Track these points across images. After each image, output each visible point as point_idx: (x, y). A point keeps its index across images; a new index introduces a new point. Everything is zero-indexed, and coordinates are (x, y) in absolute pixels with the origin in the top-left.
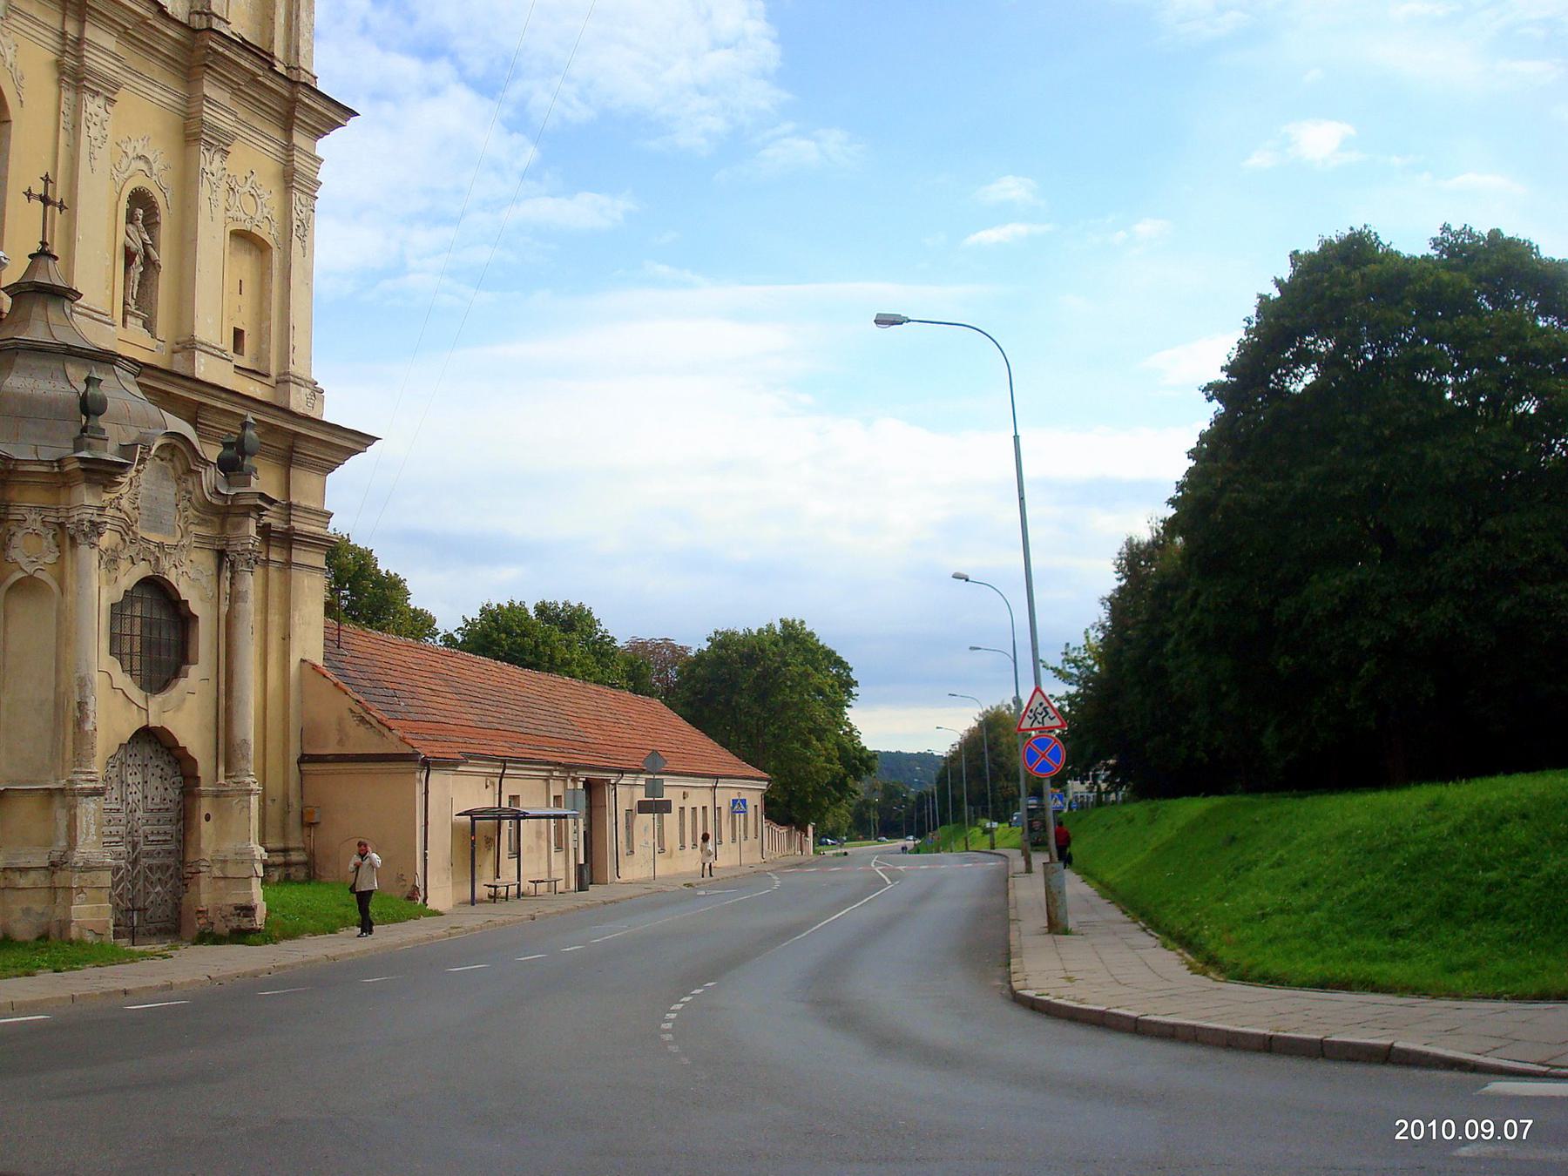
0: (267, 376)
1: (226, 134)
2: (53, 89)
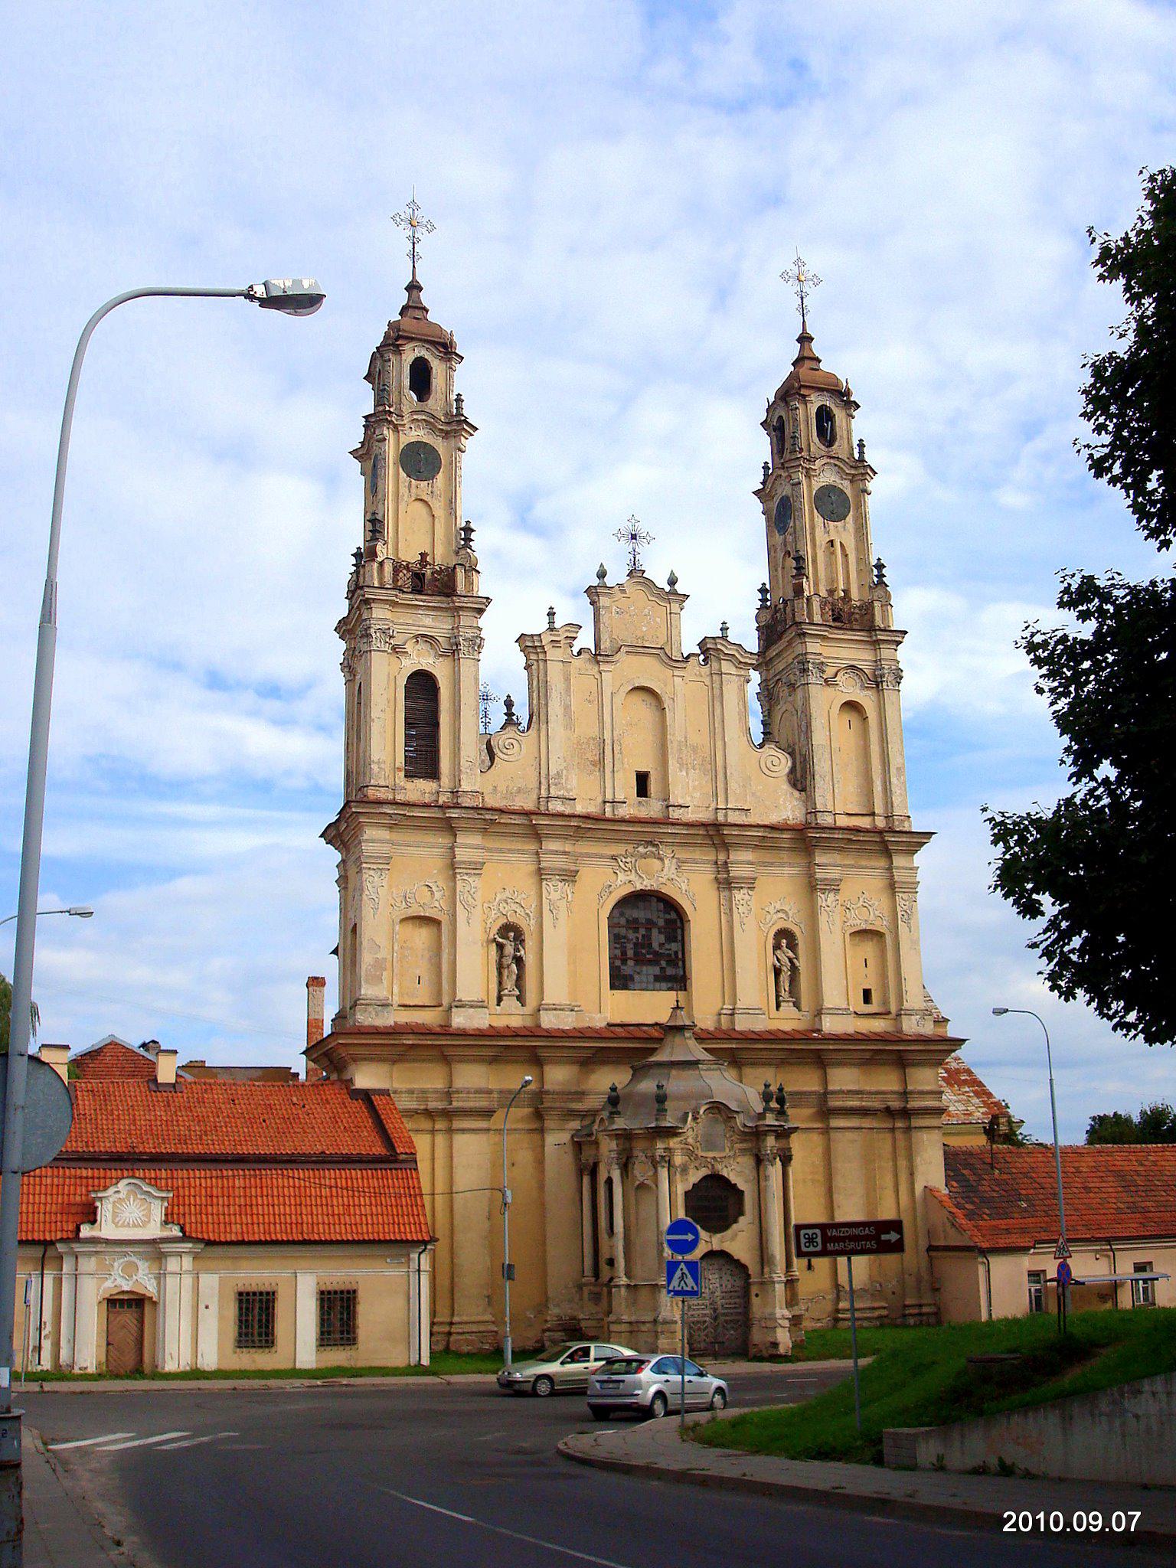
0: (889, 1013)
1: (836, 880)
2: (714, 894)
